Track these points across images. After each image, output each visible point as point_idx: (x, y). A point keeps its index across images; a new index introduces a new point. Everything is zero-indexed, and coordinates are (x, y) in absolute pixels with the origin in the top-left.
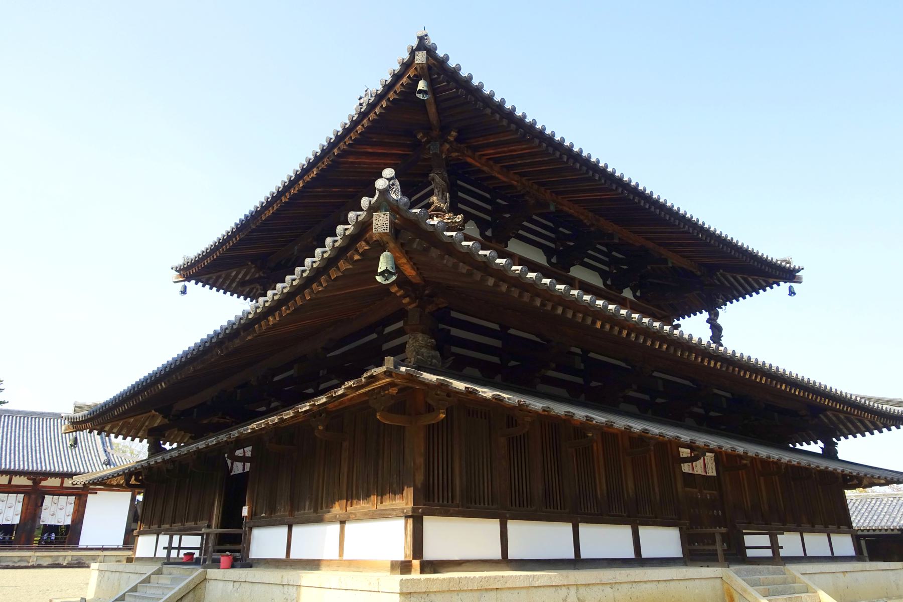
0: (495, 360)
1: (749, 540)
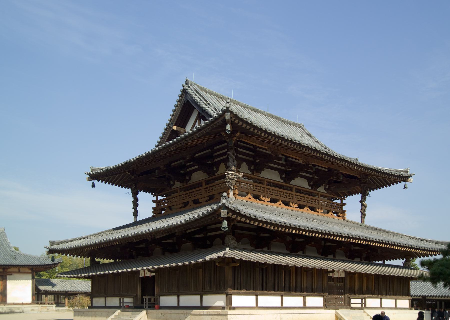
1: (353, 301)
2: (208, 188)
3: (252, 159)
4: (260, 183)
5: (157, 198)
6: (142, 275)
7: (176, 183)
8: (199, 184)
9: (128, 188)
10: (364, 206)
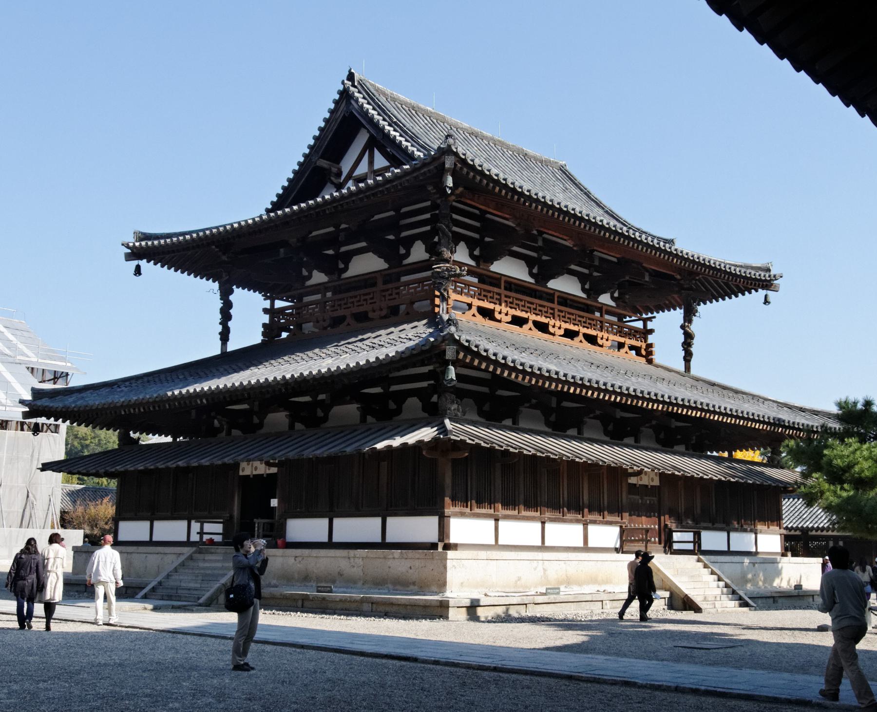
0: (485, 390)
2: (388, 290)
3: (476, 236)
4: (491, 284)
5: (272, 304)
6: (246, 470)
7: (315, 273)
8: (367, 281)
9: (214, 282)
10: (688, 338)
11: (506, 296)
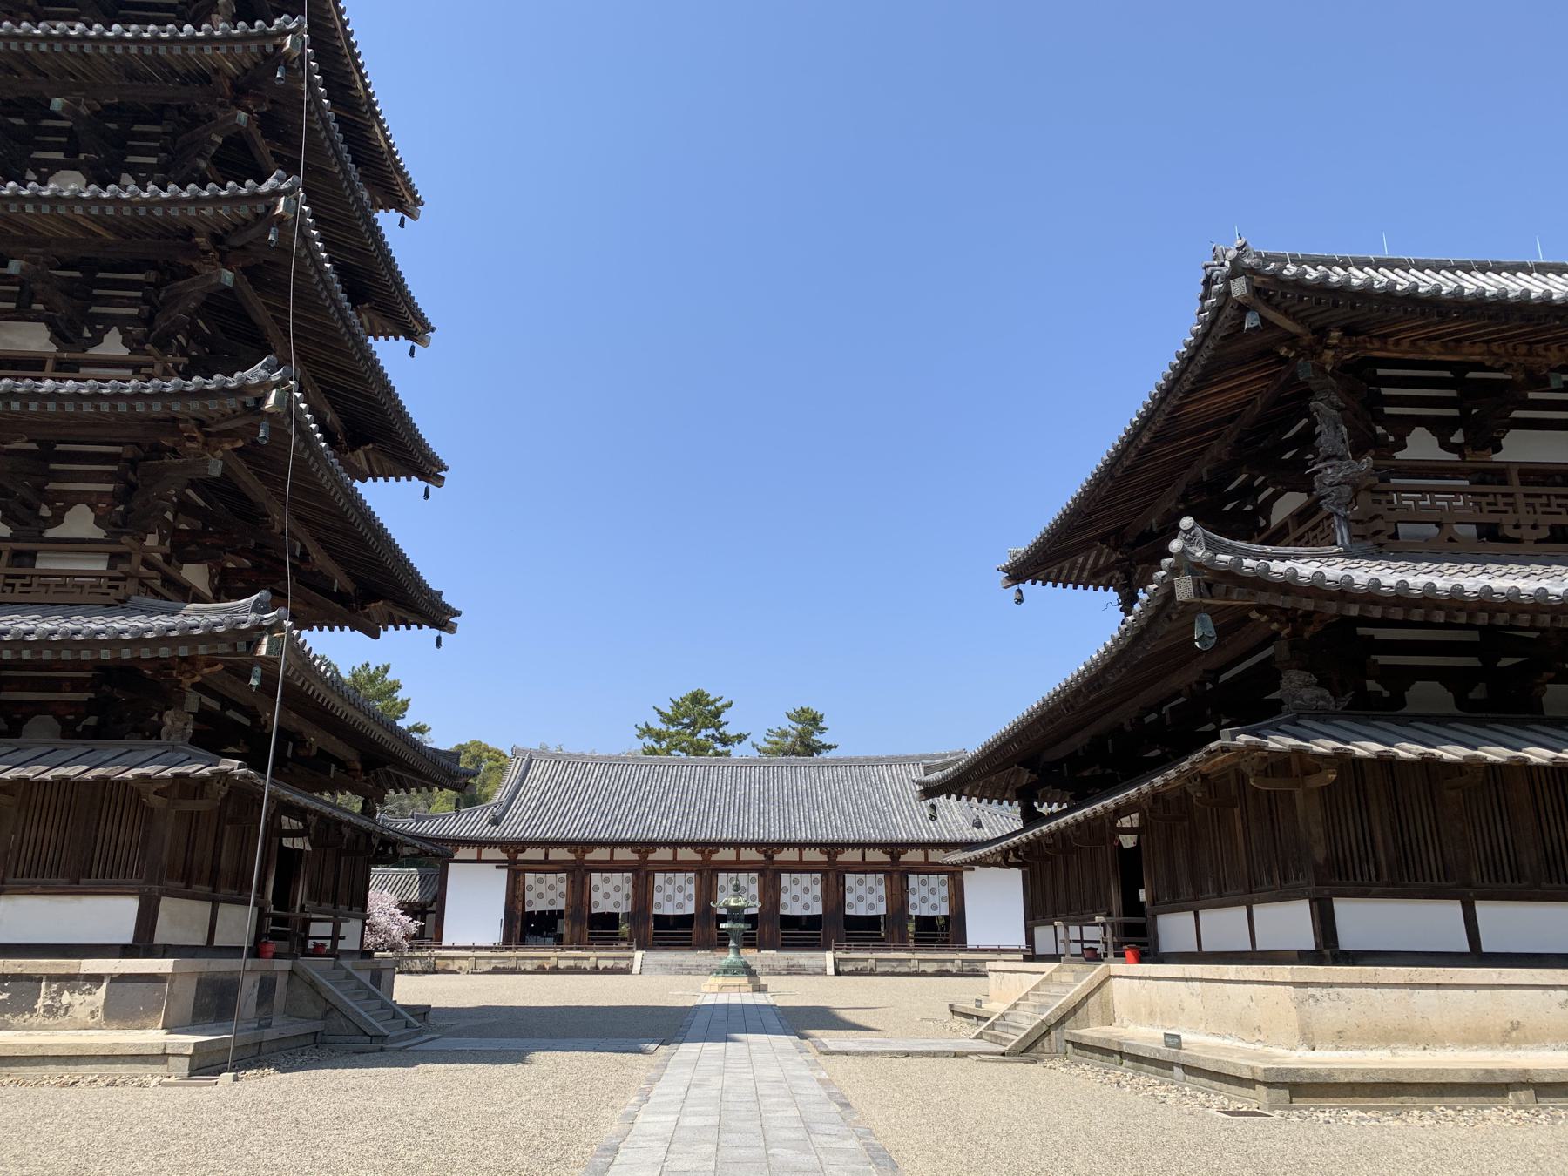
0: (1473, 661)
3: (1455, 412)
11: (1526, 495)
